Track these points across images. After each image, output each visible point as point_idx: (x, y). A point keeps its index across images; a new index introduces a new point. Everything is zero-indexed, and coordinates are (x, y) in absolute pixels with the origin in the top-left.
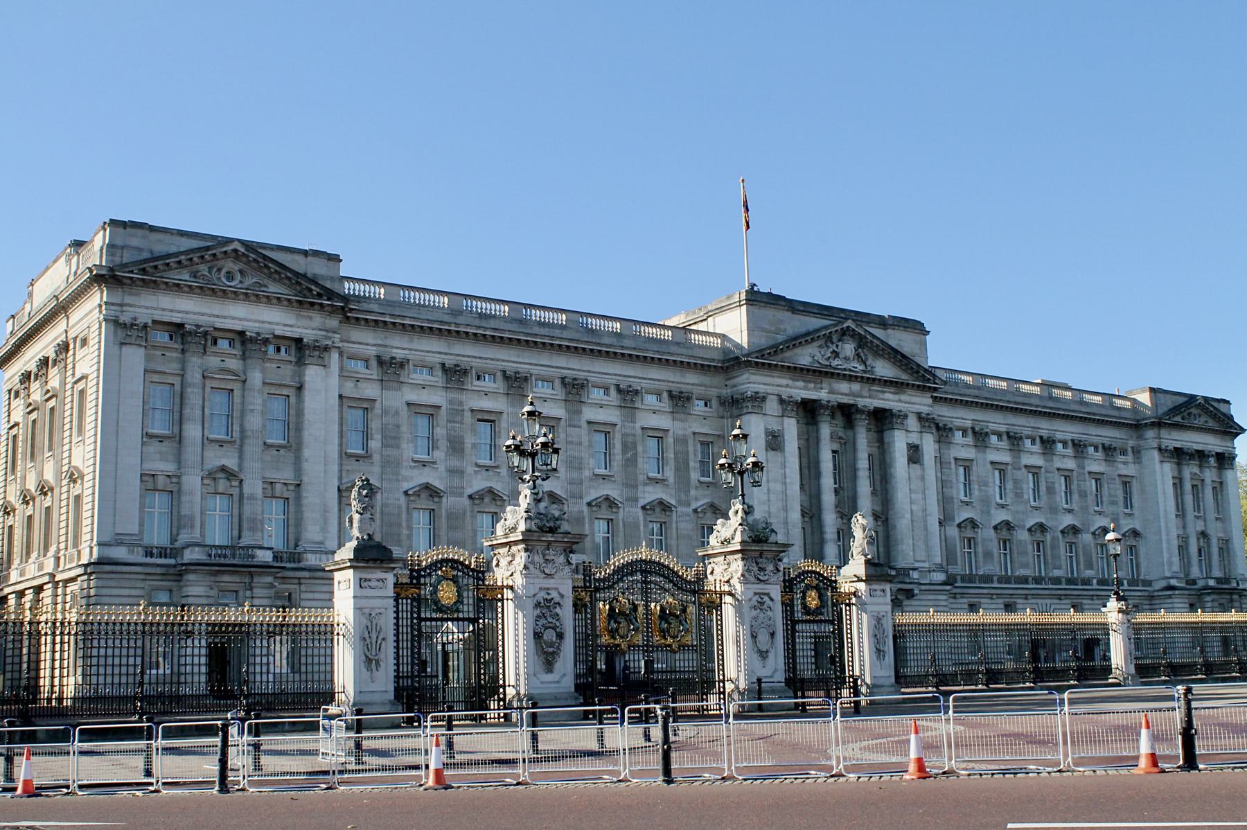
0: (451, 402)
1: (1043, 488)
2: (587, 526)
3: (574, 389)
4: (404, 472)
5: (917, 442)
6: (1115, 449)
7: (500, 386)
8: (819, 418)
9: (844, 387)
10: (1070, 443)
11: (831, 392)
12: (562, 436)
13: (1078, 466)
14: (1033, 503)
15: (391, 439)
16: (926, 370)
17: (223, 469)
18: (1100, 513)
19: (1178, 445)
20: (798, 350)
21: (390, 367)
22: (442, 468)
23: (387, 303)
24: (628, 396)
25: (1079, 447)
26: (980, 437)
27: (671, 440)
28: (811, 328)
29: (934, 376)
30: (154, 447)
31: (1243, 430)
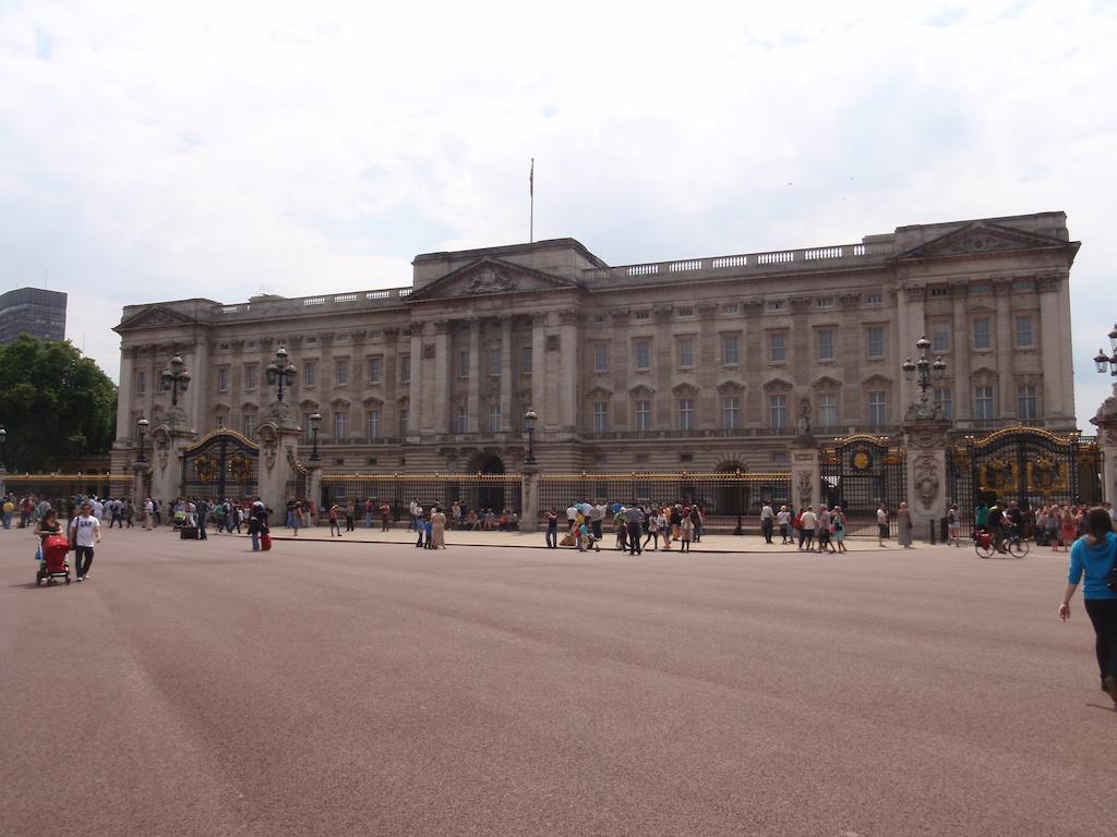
0: (263, 359)
1: (743, 348)
4: (242, 398)
5: (556, 333)
6: (857, 298)
9: (488, 305)
11: (476, 310)
13: (796, 323)
15: (236, 383)
16: (556, 277)
18: (826, 364)
19: (943, 279)
22: (258, 393)
24: (359, 338)
25: (799, 306)
26: (664, 316)
27: (384, 360)
30: (139, 400)
31: (1079, 244)
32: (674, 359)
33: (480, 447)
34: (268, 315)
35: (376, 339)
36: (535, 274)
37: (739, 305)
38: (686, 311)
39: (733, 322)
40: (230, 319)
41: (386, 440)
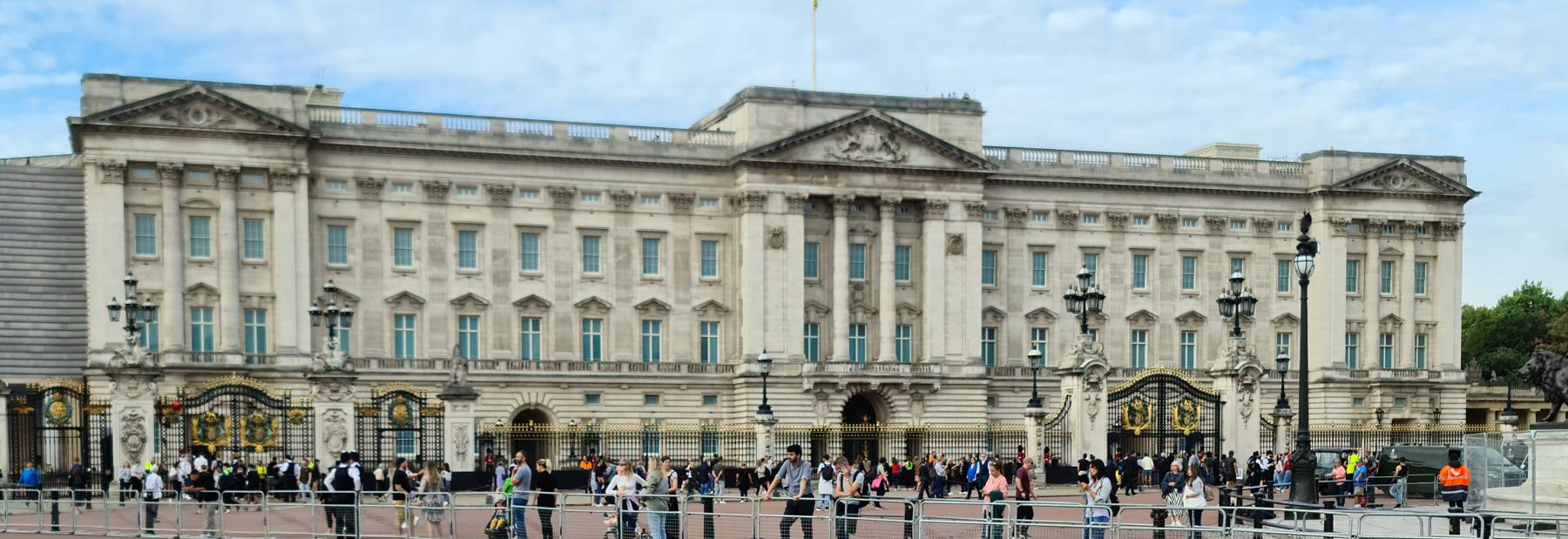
0: (431, 216)
3: (563, 198)
6: (1270, 224)
7: (480, 197)
8: (837, 213)
9: (867, 179)
10: (1201, 220)
12: (550, 242)
13: (1211, 245)
15: (371, 252)
17: (201, 286)
19: (1363, 215)
21: (371, 188)
23: (367, 128)
24: (623, 201)
25: (1215, 225)
26: (1068, 220)
28: (830, 120)
29: (983, 162)
33: (875, 383)
34: (438, 139)
35: (650, 206)
37: (1152, 219)
38: (1094, 216)
39: (1144, 236)
40: (350, 133)
41: (684, 368)
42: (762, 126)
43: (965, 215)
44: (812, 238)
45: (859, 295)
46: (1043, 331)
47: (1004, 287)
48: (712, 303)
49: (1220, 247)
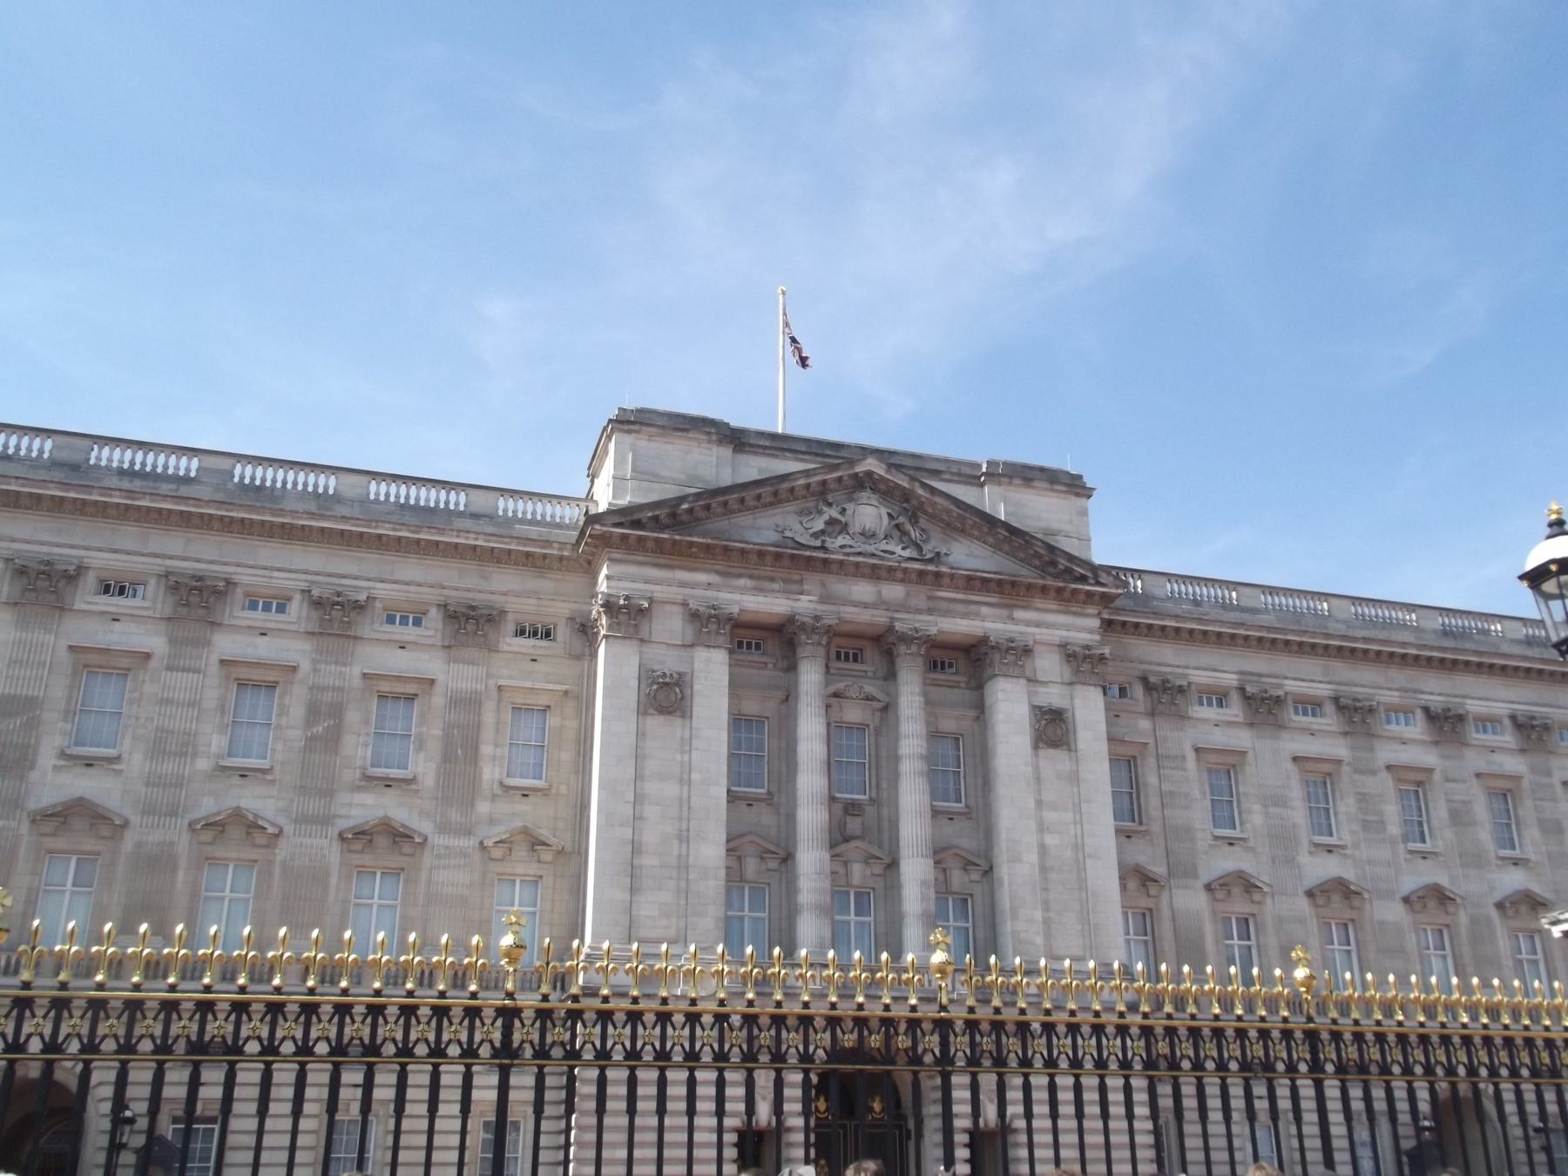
1: (1439, 812)
2: (181, 876)
8: (801, 652)
9: (862, 590)
10: (1507, 722)
12: (149, 688)
13: (1533, 769)
14: (1412, 846)
16: (1071, 558)
20: (744, 520)
24: (337, 614)
26: (1264, 707)
32: (1298, 815)
35: (410, 633)
36: (1010, 537)
37: (1419, 714)
38: (1311, 705)
39: (1408, 743)
42: (642, 473)
43: (1067, 676)
44: (751, 707)
45: (854, 825)
46: (1244, 922)
47: (1156, 827)
48: (525, 831)
49: (1549, 774)
